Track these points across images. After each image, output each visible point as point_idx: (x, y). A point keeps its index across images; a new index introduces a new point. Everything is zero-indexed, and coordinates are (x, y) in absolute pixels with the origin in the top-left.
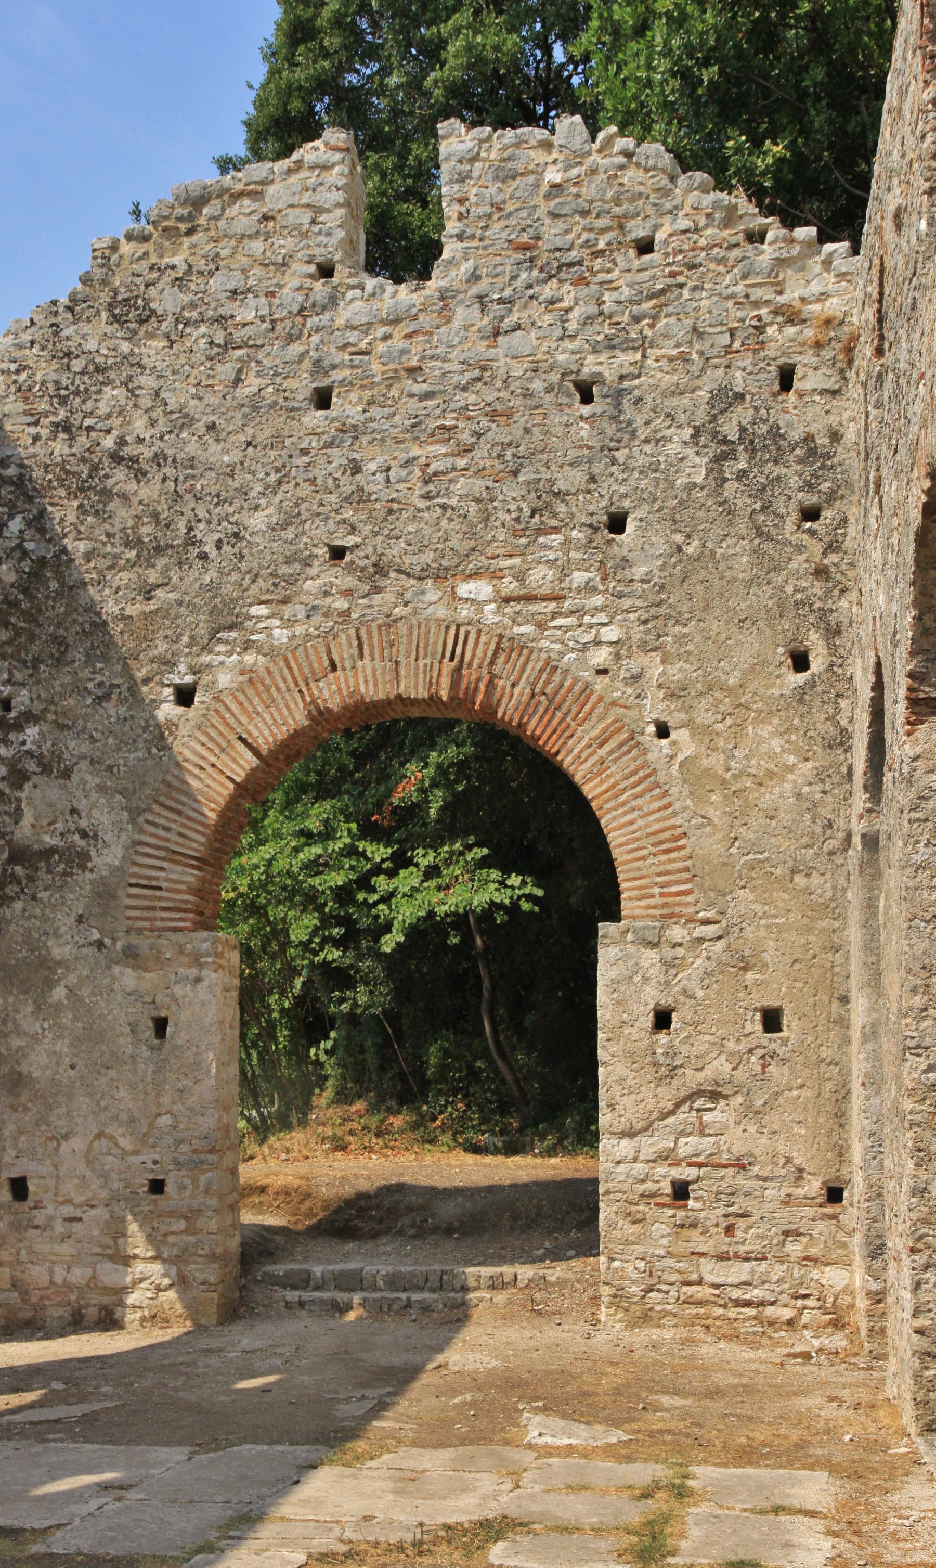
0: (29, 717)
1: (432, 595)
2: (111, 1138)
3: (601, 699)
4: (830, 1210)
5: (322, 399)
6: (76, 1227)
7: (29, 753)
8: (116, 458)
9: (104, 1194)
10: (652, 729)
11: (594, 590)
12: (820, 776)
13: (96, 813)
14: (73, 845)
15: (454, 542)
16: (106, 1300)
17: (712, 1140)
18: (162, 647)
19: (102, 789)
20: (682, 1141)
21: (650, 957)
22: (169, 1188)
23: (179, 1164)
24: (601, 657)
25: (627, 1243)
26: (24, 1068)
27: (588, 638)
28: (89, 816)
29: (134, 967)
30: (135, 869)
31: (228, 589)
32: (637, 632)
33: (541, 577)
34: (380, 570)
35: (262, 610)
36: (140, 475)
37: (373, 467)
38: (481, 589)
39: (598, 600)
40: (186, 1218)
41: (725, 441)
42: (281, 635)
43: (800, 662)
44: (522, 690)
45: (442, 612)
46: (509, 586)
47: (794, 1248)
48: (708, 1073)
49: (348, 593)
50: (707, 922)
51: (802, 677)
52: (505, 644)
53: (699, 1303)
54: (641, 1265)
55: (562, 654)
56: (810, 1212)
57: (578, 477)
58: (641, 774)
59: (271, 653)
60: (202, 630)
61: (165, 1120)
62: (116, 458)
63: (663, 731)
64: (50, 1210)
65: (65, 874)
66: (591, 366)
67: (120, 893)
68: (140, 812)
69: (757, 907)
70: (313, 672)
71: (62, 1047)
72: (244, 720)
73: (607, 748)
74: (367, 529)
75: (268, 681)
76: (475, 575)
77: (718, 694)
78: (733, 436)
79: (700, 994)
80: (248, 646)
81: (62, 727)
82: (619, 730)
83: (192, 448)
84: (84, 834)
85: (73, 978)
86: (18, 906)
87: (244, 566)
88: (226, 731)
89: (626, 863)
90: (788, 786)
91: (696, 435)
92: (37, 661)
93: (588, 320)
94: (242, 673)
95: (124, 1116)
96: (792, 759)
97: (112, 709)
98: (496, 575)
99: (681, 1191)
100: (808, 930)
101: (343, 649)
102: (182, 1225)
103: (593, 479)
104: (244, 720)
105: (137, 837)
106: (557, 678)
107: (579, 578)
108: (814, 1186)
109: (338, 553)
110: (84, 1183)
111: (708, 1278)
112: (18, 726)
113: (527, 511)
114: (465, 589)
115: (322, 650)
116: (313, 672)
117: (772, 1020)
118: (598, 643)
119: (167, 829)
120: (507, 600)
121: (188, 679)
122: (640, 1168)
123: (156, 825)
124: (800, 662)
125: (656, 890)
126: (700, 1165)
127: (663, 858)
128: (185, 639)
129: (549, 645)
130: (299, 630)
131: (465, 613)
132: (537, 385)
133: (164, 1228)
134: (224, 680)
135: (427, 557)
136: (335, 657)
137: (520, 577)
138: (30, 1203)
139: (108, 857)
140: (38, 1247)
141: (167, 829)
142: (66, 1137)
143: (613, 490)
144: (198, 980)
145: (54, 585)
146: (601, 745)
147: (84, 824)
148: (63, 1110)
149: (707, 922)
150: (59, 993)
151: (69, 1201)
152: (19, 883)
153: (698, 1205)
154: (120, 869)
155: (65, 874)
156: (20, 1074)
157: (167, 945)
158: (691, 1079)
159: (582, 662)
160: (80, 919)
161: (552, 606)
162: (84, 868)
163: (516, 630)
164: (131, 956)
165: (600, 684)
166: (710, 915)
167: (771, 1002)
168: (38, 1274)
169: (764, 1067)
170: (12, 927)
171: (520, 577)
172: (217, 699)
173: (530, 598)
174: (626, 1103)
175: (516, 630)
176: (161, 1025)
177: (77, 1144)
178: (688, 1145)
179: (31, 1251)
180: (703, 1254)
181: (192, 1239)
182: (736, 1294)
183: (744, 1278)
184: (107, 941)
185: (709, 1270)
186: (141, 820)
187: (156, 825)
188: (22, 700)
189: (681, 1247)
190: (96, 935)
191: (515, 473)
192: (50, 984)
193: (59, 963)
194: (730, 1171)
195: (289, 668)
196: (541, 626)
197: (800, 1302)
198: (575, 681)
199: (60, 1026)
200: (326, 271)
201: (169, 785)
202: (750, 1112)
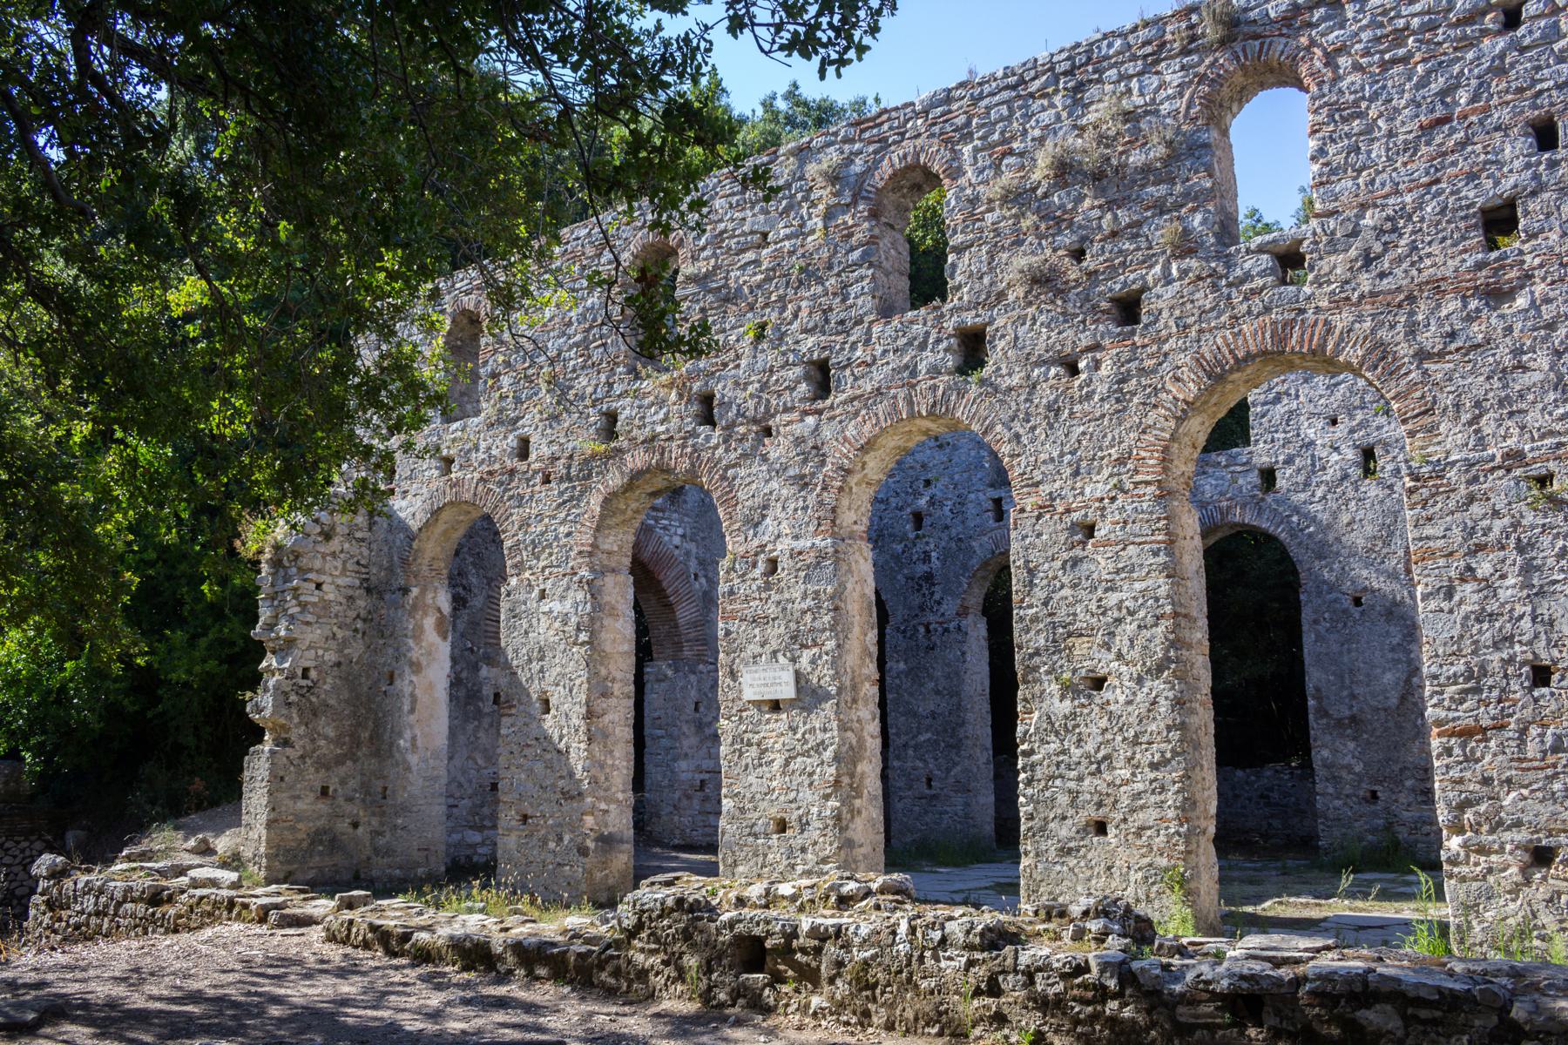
6: (455, 810)
9: (470, 791)
16: (468, 852)
21: (692, 678)
24: (677, 540)
122: (690, 775)
196: (656, 520)
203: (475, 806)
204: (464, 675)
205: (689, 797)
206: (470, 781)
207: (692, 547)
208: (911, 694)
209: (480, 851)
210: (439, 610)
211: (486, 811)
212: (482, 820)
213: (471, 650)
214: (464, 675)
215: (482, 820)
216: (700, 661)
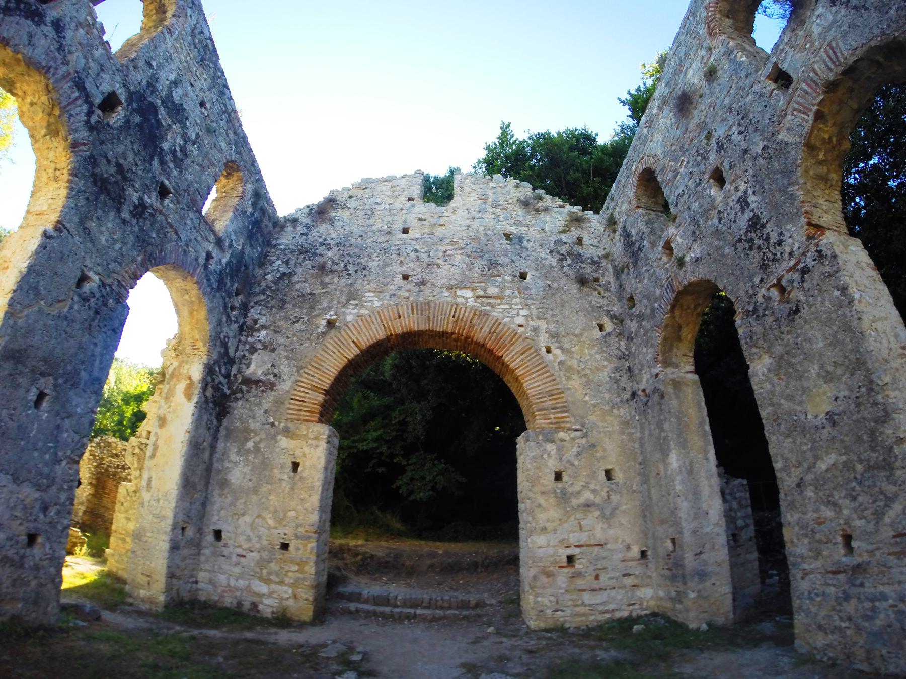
0: (264, 327)
1: (446, 294)
2: (264, 519)
3: (520, 336)
4: (642, 562)
5: (405, 231)
6: (243, 560)
7: (260, 341)
8: (322, 244)
9: (258, 546)
10: (544, 349)
11: (516, 297)
12: (617, 369)
13: (282, 367)
14: (269, 380)
15: (456, 277)
17: (587, 533)
18: (325, 304)
19: (287, 357)
20: (571, 535)
22: (291, 548)
23: (297, 537)
24: (520, 320)
25: (544, 588)
26: (229, 477)
27: (515, 312)
28: (279, 368)
29: (287, 437)
30: (296, 392)
31: (358, 286)
32: (534, 312)
33: (492, 290)
34: (423, 283)
35: (371, 294)
36: (329, 249)
37: (423, 251)
38: (468, 293)
39: (518, 300)
40: (298, 565)
41: (562, 254)
42: (377, 304)
43: (601, 327)
44: (486, 329)
45: (449, 299)
46: (481, 293)
47: (628, 581)
48: (582, 500)
49: (409, 291)
50: (576, 430)
51: (604, 333)
52: (477, 313)
53: (584, 615)
54: (552, 598)
55: (503, 318)
56: (634, 563)
57: (507, 260)
58: (541, 366)
59: (372, 310)
60: (343, 300)
61: (292, 514)
62: (322, 244)
63: (549, 351)
64: (231, 549)
65: (263, 391)
66: (510, 229)
67: (286, 402)
68: (302, 368)
69: (600, 424)
70: (390, 318)
71: (247, 470)
72: (356, 333)
73: (525, 355)
74: (419, 270)
75: (369, 320)
76: (466, 288)
77: (572, 337)
78: (565, 253)
79: (576, 463)
80: (363, 306)
81: (275, 332)
82: (530, 348)
83: (353, 241)
84: (275, 376)
85: (257, 439)
86: (240, 403)
87: (366, 278)
88: (347, 338)
89: (536, 403)
90: (605, 373)
91: (551, 252)
92: (273, 307)
93: (507, 218)
94: (358, 316)
95: (272, 509)
96: (605, 363)
97: (298, 326)
98: (474, 289)
99: (570, 559)
100: (623, 433)
101: (404, 310)
102: (296, 568)
103: (512, 261)
104: (356, 333)
105: (299, 378)
106: (501, 327)
107: (508, 292)
108: (635, 551)
109: (405, 277)
110: (249, 539)
111: (587, 602)
112: (259, 331)
113: (486, 269)
114: (459, 293)
115: (395, 310)
116: (390, 318)
117: (608, 474)
118: (518, 315)
119: (312, 376)
120: (478, 297)
121: (334, 317)
122: (550, 551)
123: (308, 374)
124: (601, 327)
125: (552, 416)
126: (581, 546)
127: (554, 402)
128: (335, 302)
129: (495, 314)
130: (385, 302)
131: (460, 300)
132: (489, 233)
133: (287, 568)
134: (349, 318)
135: (445, 281)
136: (401, 313)
137: (485, 291)
138: (222, 543)
139: (285, 386)
140: (224, 566)
141: (312, 376)
142: (243, 515)
143: (523, 265)
144: (317, 446)
145: (287, 282)
146: (522, 354)
147: (276, 371)
148: (243, 501)
149: (576, 430)
150: (250, 444)
151: (240, 546)
152: (242, 392)
153: (581, 566)
154: (288, 392)
155: (263, 391)
156: (226, 480)
157: (303, 429)
158: (575, 502)
159: (512, 322)
160: (266, 412)
161: (498, 301)
162: (272, 389)
163: (483, 308)
164: (287, 432)
165: (520, 330)
166: (577, 427)
167: (609, 467)
168: (222, 579)
169: (608, 497)
170: (235, 412)
171: (485, 291)
172: (346, 325)
173: (489, 297)
174: (542, 517)
175: (483, 308)
176: (296, 466)
177: (247, 519)
178: (574, 538)
179: (220, 568)
180: (584, 591)
181: (301, 576)
182: (600, 608)
183: (605, 599)
184: (276, 423)
185: (587, 598)
186: (302, 371)
187: (308, 374)
188: (263, 321)
189: (573, 587)
190: (271, 420)
191: (482, 257)
192: (247, 439)
193: (252, 431)
194: (597, 548)
195: (380, 316)
197: (631, 607)
198: (509, 329)
199: (247, 459)
200: (411, 199)
201: (318, 358)
202: (603, 516)
203: (262, 559)
204: (262, 445)
205: (549, 575)
206: (259, 537)
207: (543, 325)
208: (791, 398)
209: (266, 601)
210: (190, 378)
211: (274, 566)
212: (269, 574)
213: (273, 424)
214: (262, 445)
215: (269, 574)
216: (558, 429)
